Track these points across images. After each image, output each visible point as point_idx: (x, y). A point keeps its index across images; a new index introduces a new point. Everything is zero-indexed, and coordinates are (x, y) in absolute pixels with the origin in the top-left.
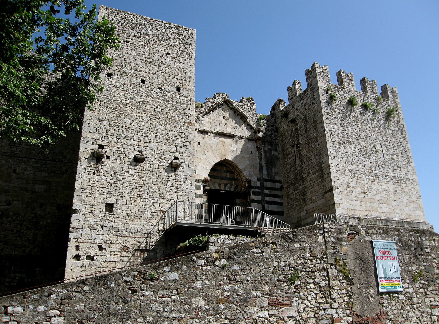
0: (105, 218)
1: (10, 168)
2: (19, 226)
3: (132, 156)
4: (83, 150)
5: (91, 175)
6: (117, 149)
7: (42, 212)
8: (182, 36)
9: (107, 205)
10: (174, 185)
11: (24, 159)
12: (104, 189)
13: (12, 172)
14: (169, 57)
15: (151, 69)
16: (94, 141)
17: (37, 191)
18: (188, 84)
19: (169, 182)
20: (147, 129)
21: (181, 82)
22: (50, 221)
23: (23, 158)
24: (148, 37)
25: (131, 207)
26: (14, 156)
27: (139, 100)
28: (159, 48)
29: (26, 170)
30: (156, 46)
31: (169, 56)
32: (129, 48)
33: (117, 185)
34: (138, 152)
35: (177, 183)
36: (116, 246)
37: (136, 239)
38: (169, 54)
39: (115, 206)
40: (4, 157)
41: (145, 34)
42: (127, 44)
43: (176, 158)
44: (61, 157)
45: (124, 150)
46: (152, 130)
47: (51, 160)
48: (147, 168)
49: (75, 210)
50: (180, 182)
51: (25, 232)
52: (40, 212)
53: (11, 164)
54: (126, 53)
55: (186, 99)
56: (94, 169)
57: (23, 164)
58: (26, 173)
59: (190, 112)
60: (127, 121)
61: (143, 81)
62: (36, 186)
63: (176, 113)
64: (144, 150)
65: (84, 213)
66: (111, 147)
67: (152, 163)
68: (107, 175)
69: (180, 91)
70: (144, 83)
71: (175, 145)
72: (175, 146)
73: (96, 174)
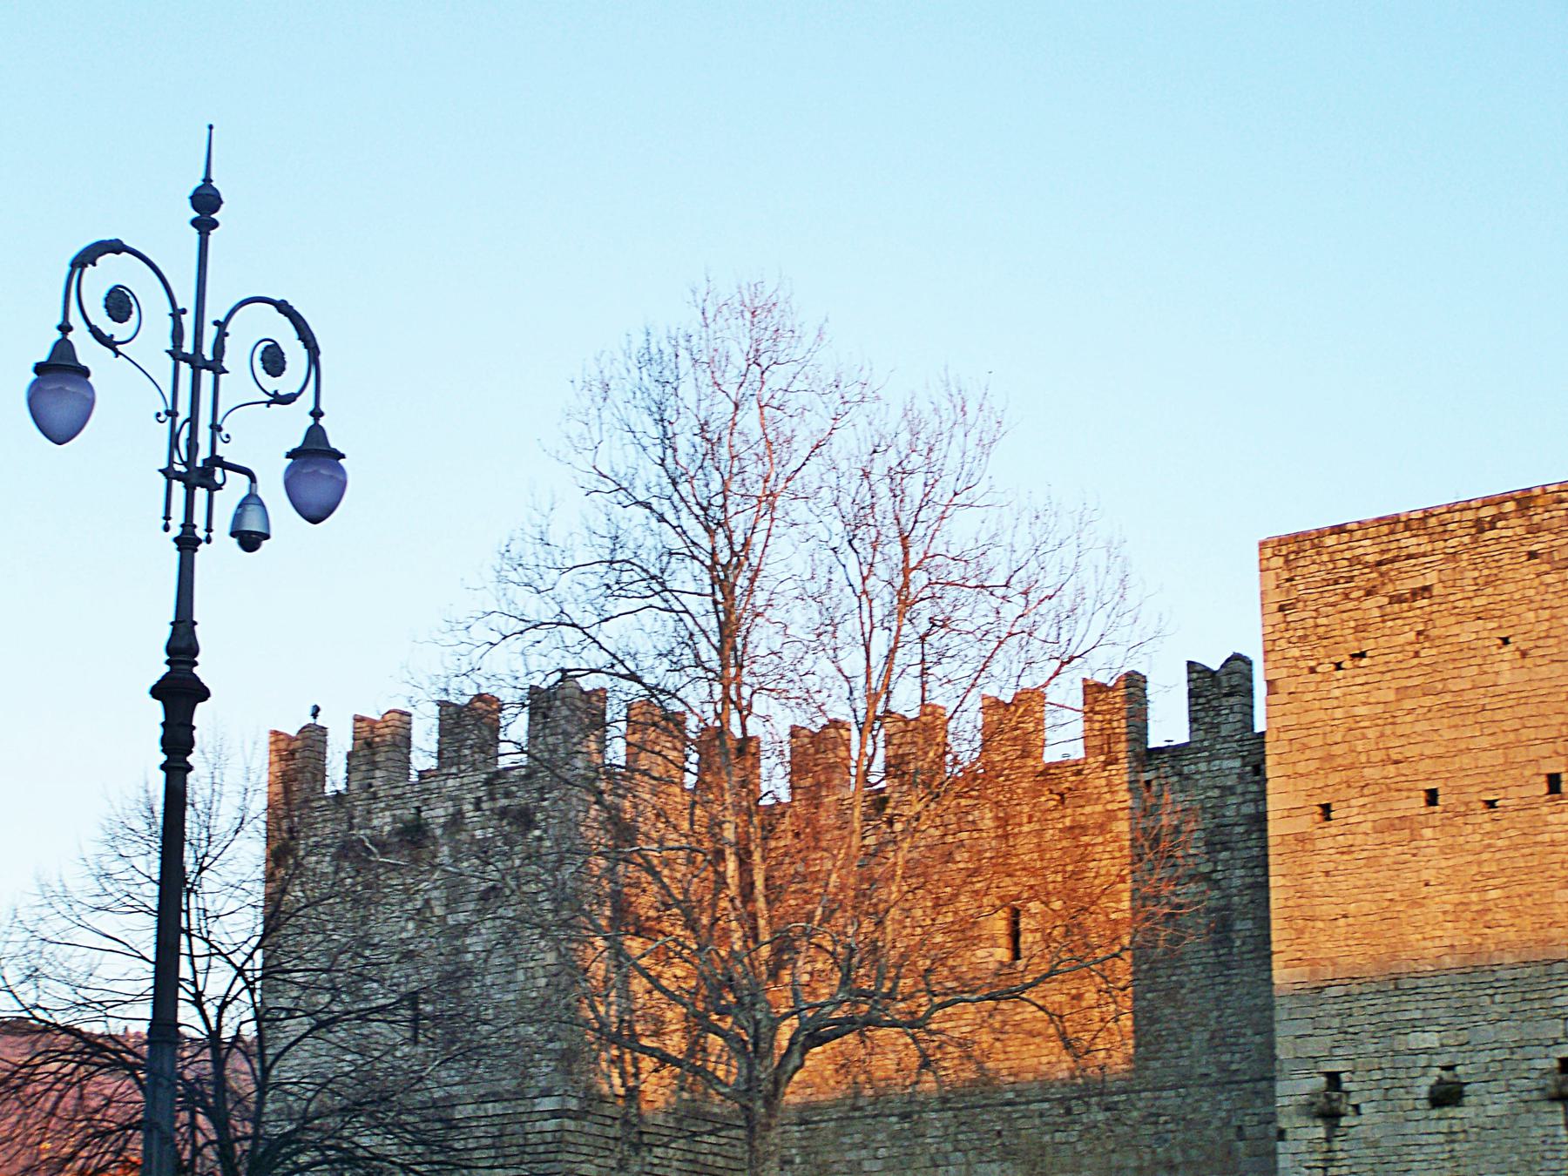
1: (1226, 1123)
3: (1424, 1086)
4: (1286, 1101)
6: (1377, 1075)
16: (1310, 1064)
20: (1461, 979)
24: (1425, 602)
26: (1231, 1083)
27: (1425, 875)
28: (1467, 632)
30: (1455, 630)
32: (1371, 678)
34: (1444, 1068)
38: (1505, 641)
40: (1204, 1090)
41: (1417, 593)
42: (1364, 662)
45: (1402, 1074)
53: (1228, 1111)
57: (1259, 1102)
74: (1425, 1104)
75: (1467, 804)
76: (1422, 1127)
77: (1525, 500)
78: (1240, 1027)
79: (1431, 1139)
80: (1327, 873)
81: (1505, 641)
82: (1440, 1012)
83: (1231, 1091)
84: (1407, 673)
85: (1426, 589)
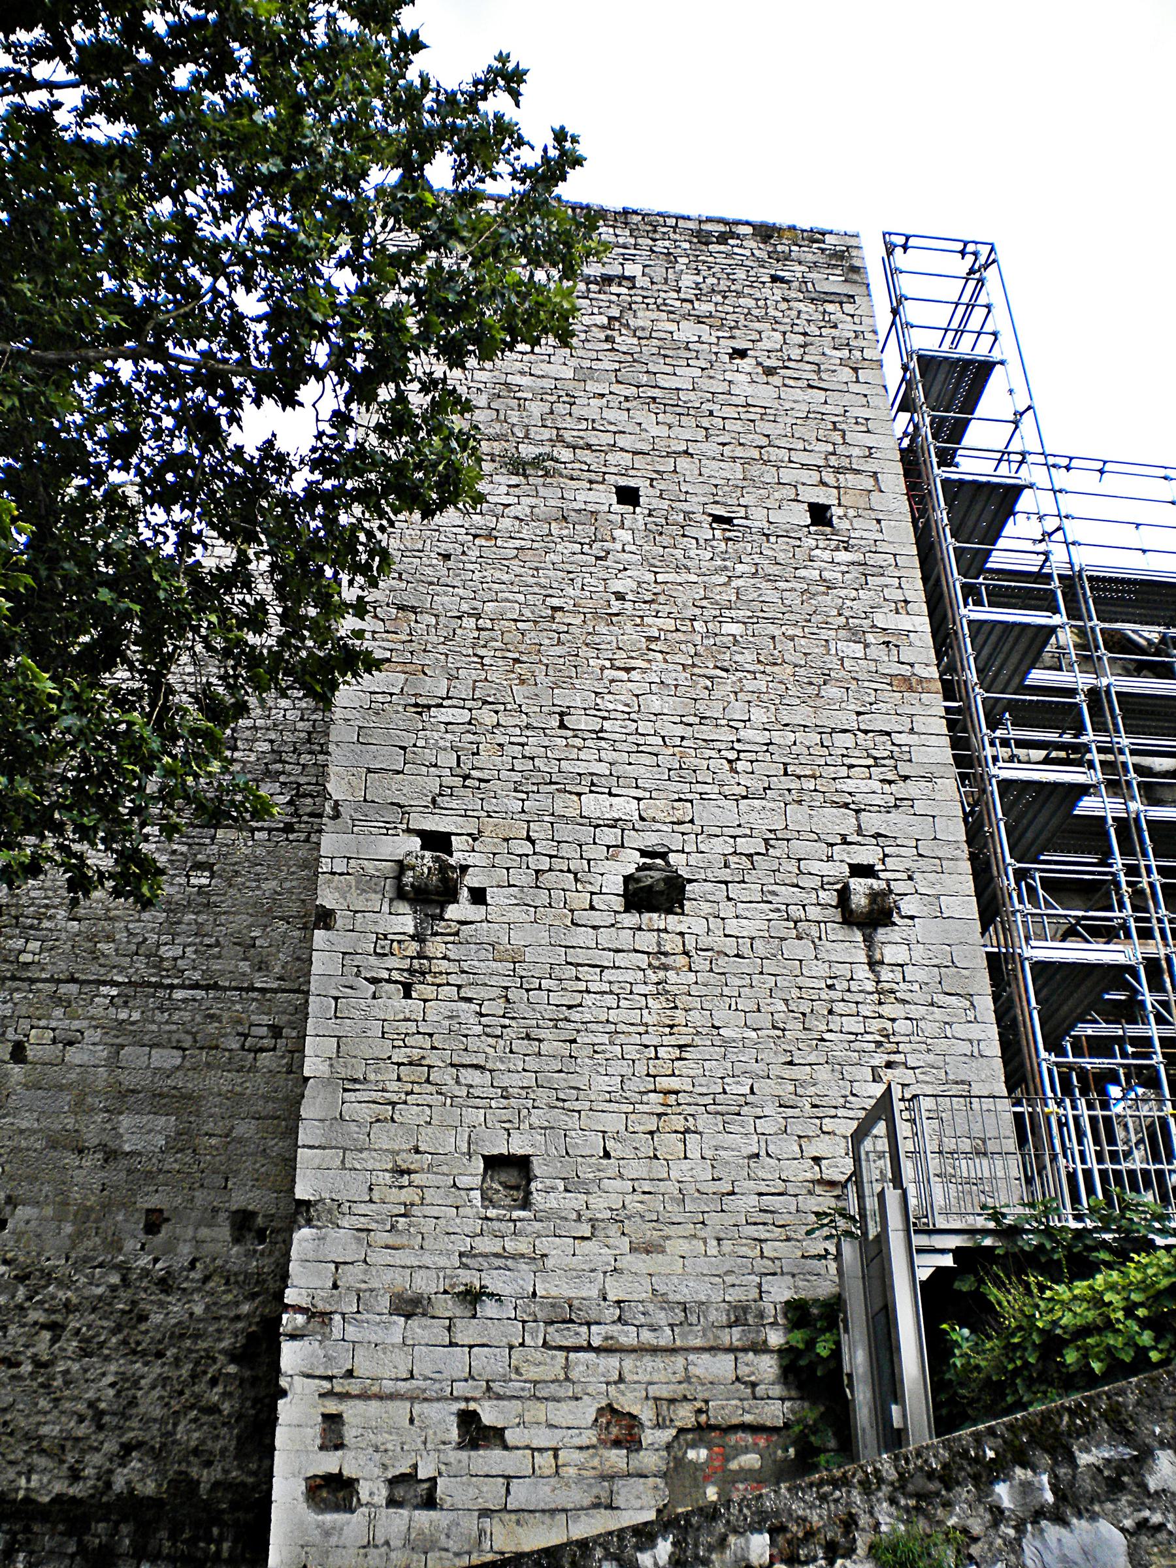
0: (486, 1245)
2: (47, 1335)
4: (340, 866)
5: (394, 1003)
7: (156, 1260)
8: (798, 268)
9: (493, 1163)
10: (875, 1025)
11: (64, 989)
12: (468, 1076)
13: (7, 1057)
14: (748, 369)
15: (663, 431)
16: (393, 815)
17: (127, 1148)
18: (869, 483)
19: (839, 1007)
20: (680, 730)
21: (829, 478)
22: (198, 1310)
23: (59, 981)
24: (624, 290)
25: (635, 1169)
26: (14, 978)
27: (617, 586)
28: (688, 331)
29: (71, 1043)
31: (746, 364)
33: (544, 1047)
34: (644, 854)
35: (886, 1010)
36: (562, 1413)
37: (680, 1361)
38: (741, 354)
39: (538, 1168)
41: (607, 280)
43: (862, 871)
44: (245, 966)
46: (707, 732)
47: (196, 986)
48: (705, 942)
49: (307, 1204)
50: (904, 1002)
51: (76, 1367)
52: (144, 1261)
54: (522, 373)
55: (872, 559)
56: (406, 964)
57: (58, 1012)
58: (74, 1055)
59: (904, 622)
60: (563, 698)
61: (628, 496)
62: (126, 1122)
63: (825, 634)
64: (676, 842)
65: (362, 1222)
66: (487, 844)
67: (727, 910)
68: (483, 993)
69: (830, 524)
70: (635, 503)
71: (849, 799)
72: (846, 806)
73: (419, 990)
74: (618, 903)
75: (687, 514)
76: (605, 937)
77: (765, 232)
78: (47, 906)
79: (620, 959)
80: (447, 557)
81: (741, 354)
82: (642, 767)
83: (13, 991)
84: (594, 355)
85: (632, 279)
